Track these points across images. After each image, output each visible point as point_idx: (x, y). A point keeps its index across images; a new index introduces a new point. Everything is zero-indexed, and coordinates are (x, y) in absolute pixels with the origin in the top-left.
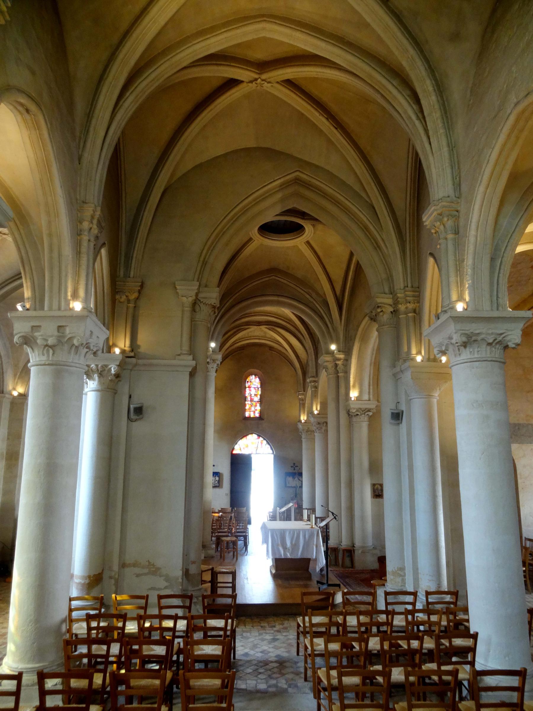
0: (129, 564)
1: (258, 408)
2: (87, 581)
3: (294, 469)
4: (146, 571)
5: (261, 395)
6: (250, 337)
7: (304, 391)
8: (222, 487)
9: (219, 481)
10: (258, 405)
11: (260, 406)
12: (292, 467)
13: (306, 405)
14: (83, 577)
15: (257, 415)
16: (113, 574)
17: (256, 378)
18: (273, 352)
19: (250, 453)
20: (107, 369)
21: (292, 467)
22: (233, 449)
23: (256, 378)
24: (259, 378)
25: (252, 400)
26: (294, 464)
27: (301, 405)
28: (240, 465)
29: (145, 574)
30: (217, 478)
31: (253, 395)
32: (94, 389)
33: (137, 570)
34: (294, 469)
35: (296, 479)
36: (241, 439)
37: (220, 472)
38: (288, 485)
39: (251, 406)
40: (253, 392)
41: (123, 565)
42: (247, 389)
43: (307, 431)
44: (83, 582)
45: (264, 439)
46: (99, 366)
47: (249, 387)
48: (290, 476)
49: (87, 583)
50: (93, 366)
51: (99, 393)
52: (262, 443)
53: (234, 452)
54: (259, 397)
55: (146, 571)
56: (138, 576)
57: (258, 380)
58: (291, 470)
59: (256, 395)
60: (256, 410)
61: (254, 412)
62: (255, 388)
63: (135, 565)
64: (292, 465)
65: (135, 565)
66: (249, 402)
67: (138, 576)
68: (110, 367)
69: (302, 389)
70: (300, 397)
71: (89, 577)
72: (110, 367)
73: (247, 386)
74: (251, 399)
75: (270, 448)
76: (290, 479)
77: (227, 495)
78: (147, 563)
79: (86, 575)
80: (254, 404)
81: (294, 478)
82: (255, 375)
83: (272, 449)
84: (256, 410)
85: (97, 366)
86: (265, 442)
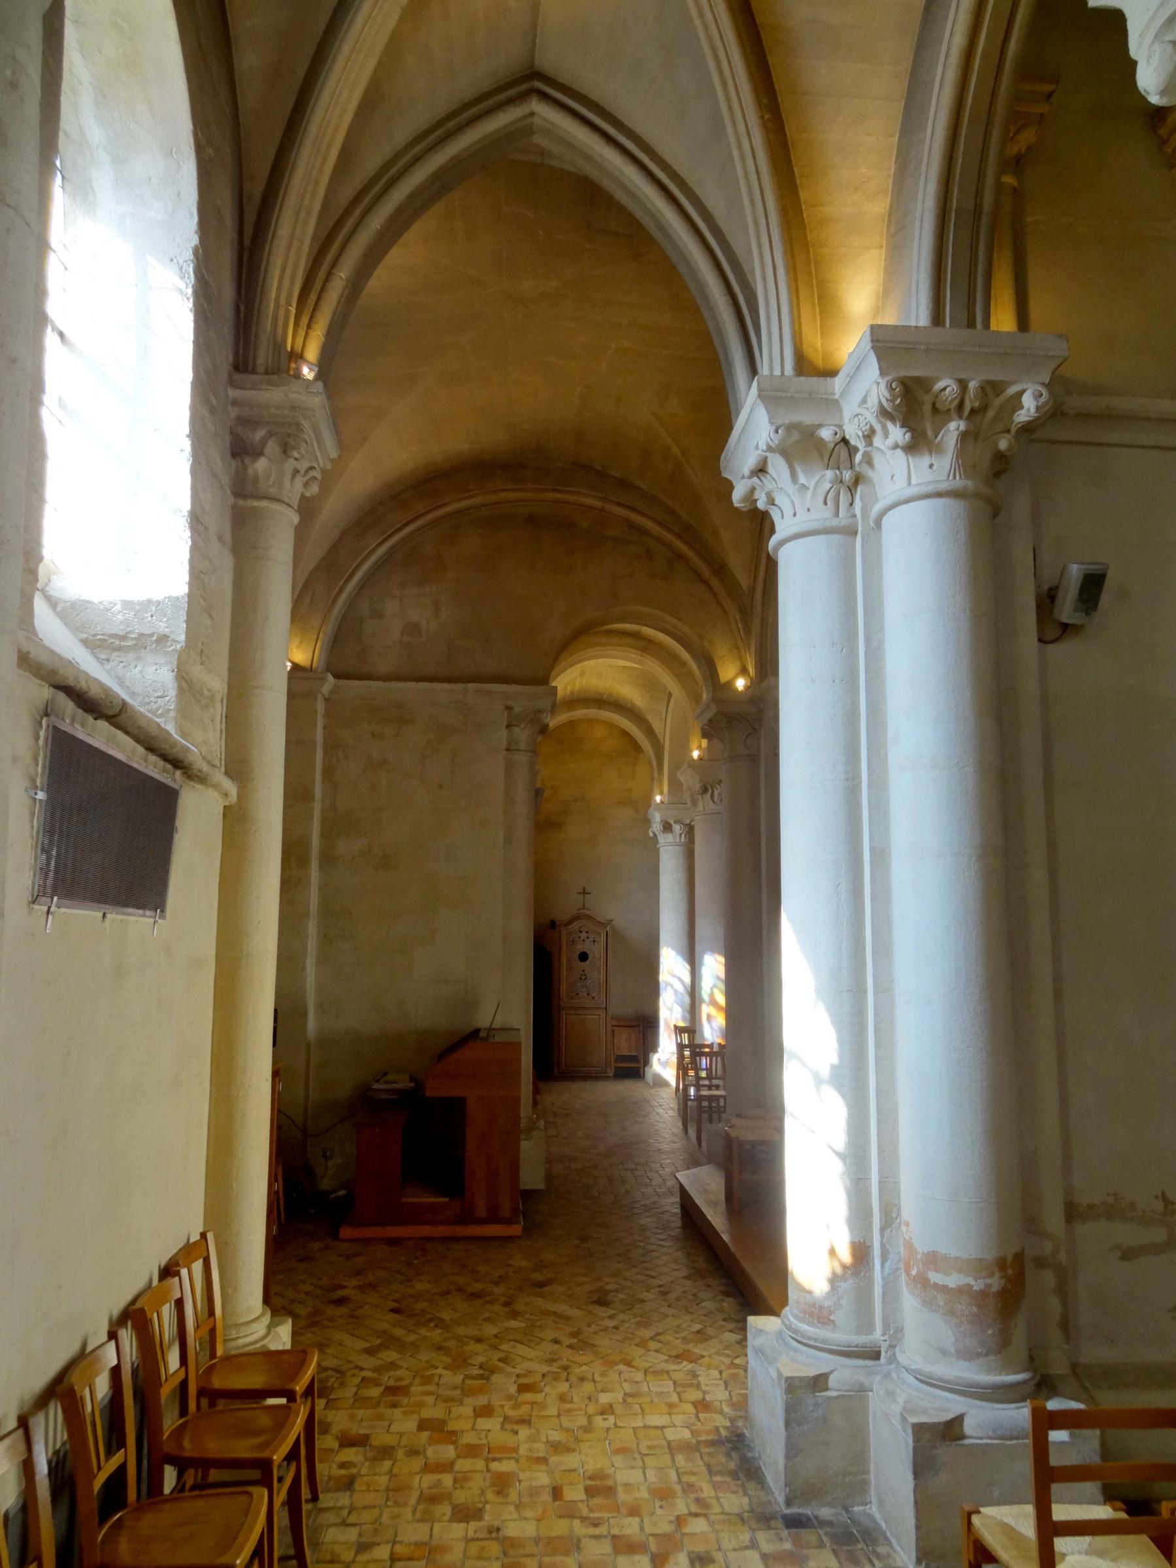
0: (1091, 1207)
2: (996, 1283)
4: (1159, 1235)
14: (977, 1267)
16: (1047, 1248)
20: (998, 402)
29: (1157, 1249)
32: (931, 488)
33: (1125, 1233)
41: (1072, 1212)
44: (978, 1285)
46: (973, 385)
49: (994, 1289)
50: (946, 386)
51: (956, 507)
55: (1159, 1235)
56: (1128, 1254)
63: (1114, 1210)
65: (1114, 1210)
67: (1128, 1254)
68: (1013, 390)
71: (1001, 1264)
72: (1013, 390)
78: (1159, 1206)
79: (989, 1256)
85: (963, 384)
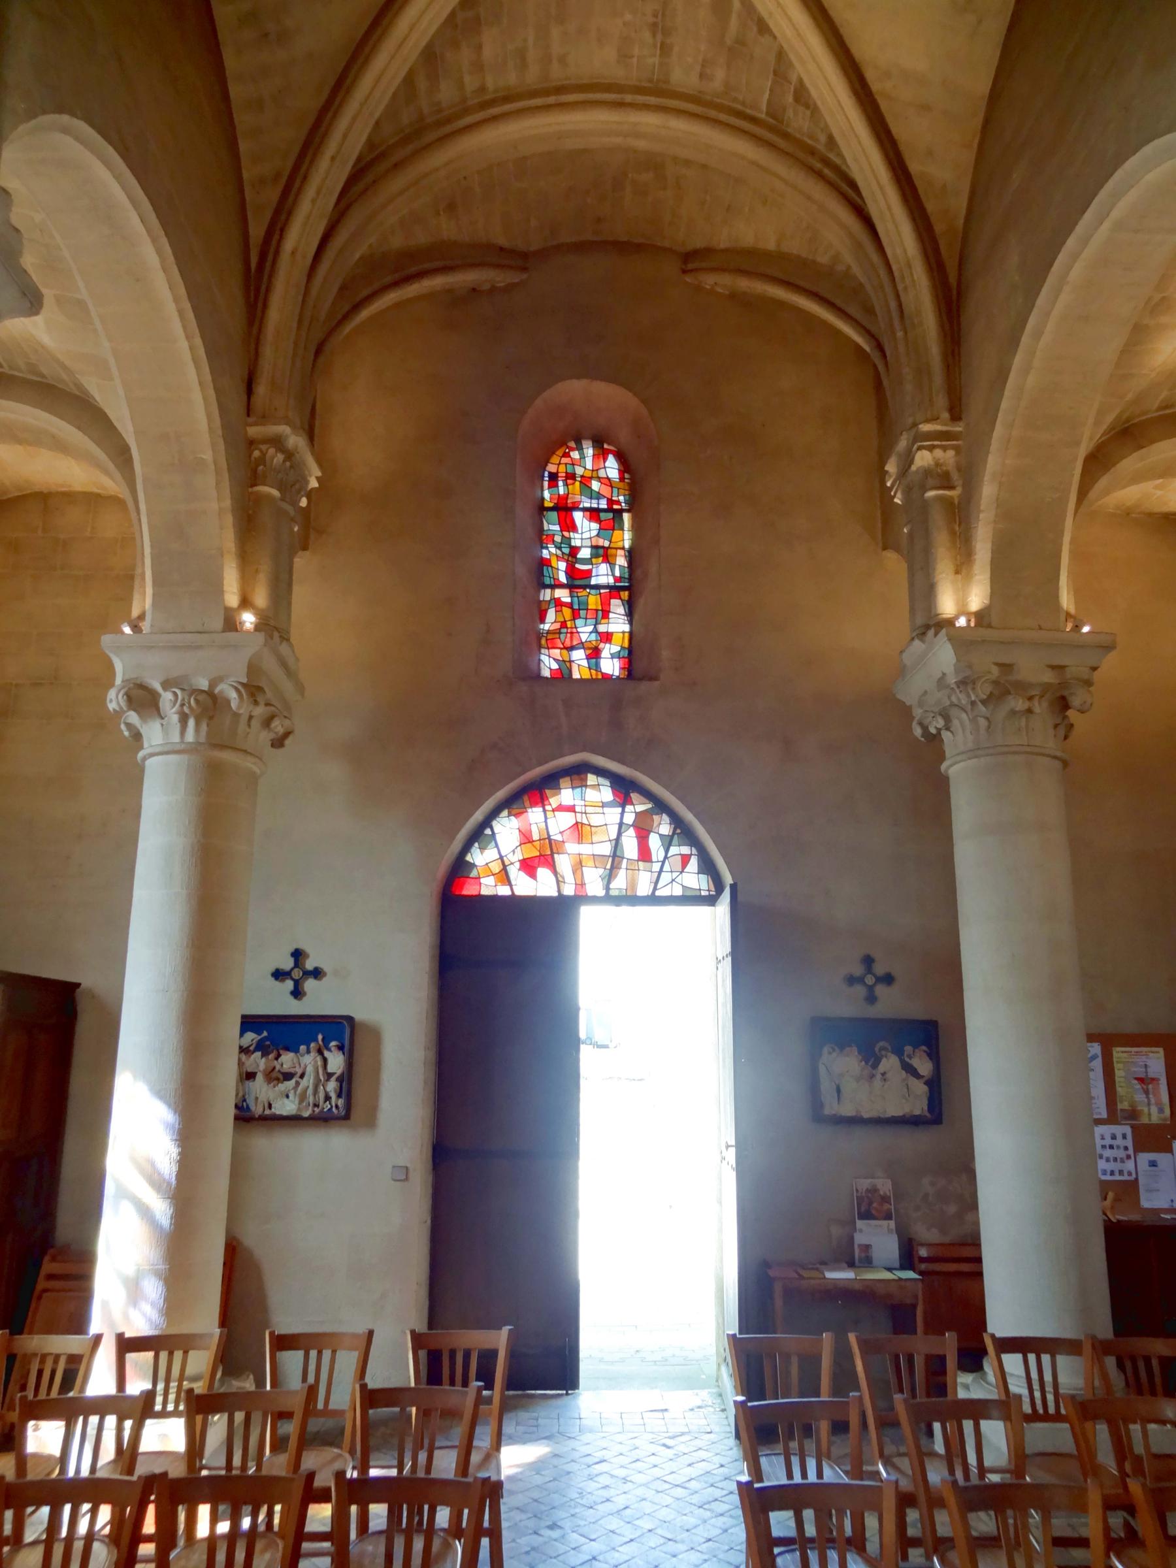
1: (618, 624)
3: (871, 999)
5: (631, 555)
6: (560, 90)
7: (956, 415)
8: (370, 1122)
9: (346, 1082)
10: (618, 608)
11: (630, 614)
12: (851, 980)
13: (988, 491)
15: (611, 666)
17: (601, 454)
18: (709, 280)
19: (569, 890)
21: (851, 980)
22: (460, 869)
23: (601, 454)
24: (621, 457)
25: (578, 579)
26: (868, 961)
27: (938, 518)
28: (494, 976)
30: (336, 1062)
31: (585, 553)
34: (871, 999)
35: (890, 1063)
36: (513, 803)
37: (358, 1016)
38: (831, 1107)
39: (576, 615)
40: (586, 531)
42: (552, 526)
43: (1004, 687)
45: (661, 807)
47: (564, 509)
48: (842, 1046)
52: (643, 836)
53: (469, 890)
54: (621, 561)
57: (612, 468)
58: (847, 1005)
59: (604, 554)
60: (607, 637)
61: (594, 654)
62: (594, 514)
64: (858, 970)
66: (563, 595)
69: (941, 401)
70: (923, 459)
73: (548, 504)
74: (571, 572)
75: (693, 864)
76: (845, 1064)
77: (403, 1174)
80: (593, 601)
81: (871, 1058)
82: (598, 443)
83: (707, 867)
84: (607, 637)
86: (664, 827)
